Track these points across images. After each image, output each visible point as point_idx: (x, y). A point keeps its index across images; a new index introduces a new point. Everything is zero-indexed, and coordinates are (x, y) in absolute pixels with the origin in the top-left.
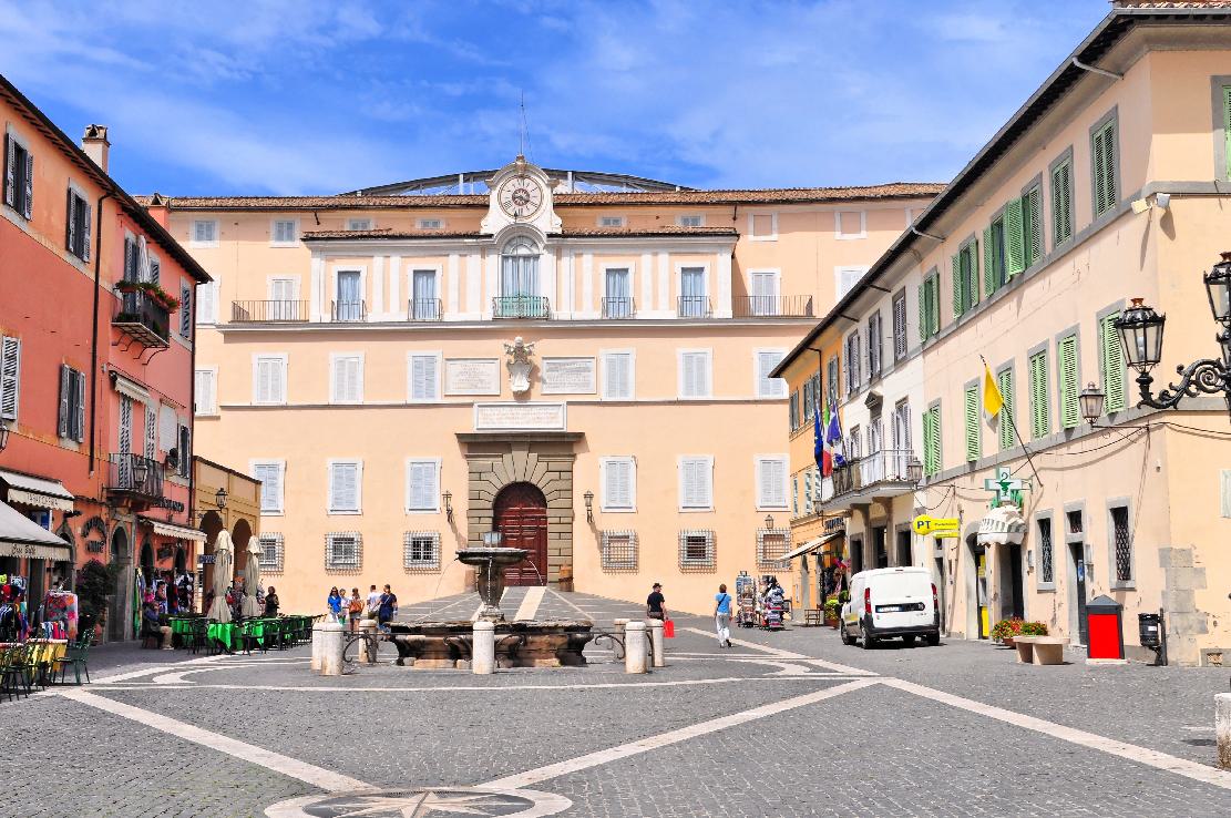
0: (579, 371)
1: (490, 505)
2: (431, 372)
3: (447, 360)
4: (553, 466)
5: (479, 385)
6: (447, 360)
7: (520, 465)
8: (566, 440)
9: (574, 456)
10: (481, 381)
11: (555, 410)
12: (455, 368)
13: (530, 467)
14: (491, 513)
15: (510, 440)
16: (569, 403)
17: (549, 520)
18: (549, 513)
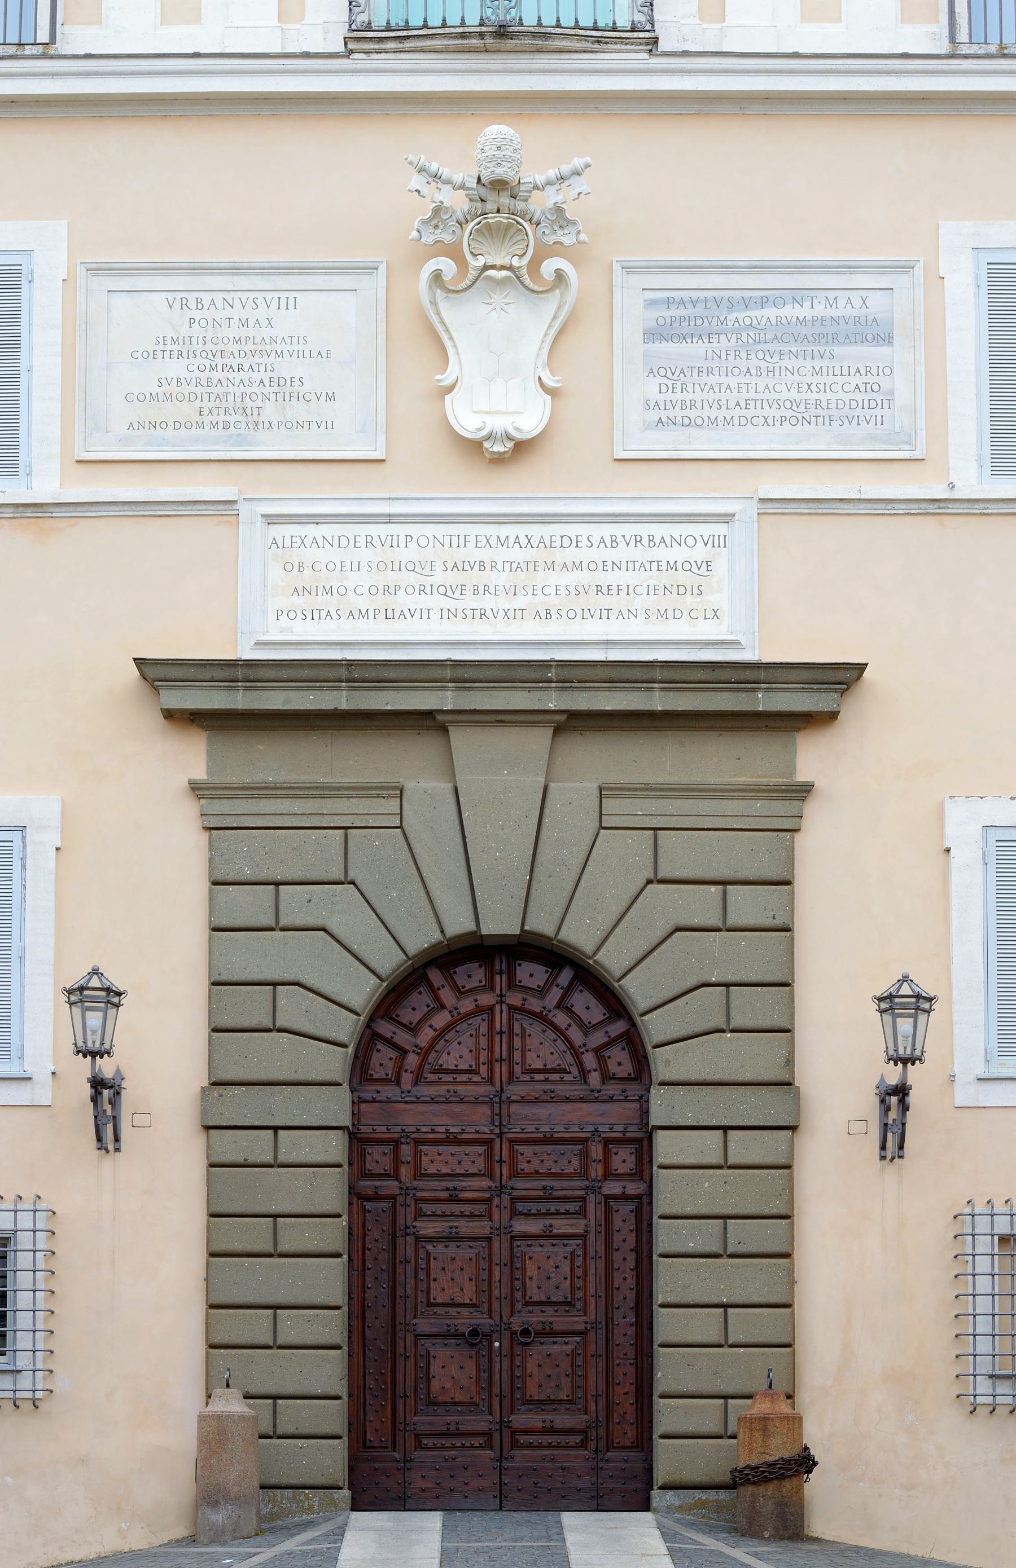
0: (826, 334)
1: (334, 1063)
3: (98, 270)
4: (681, 855)
5: (270, 411)
6: (98, 270)
7: (501, 853)
8: (763, 701)
9: (805, 791)
10: (285, 390)
11: (688, 546)
12: (141, 316)
13: (562, 852)
15: (446, 700)
16: (773, 507)
17: (667, 1147)
18: (661, 1106)
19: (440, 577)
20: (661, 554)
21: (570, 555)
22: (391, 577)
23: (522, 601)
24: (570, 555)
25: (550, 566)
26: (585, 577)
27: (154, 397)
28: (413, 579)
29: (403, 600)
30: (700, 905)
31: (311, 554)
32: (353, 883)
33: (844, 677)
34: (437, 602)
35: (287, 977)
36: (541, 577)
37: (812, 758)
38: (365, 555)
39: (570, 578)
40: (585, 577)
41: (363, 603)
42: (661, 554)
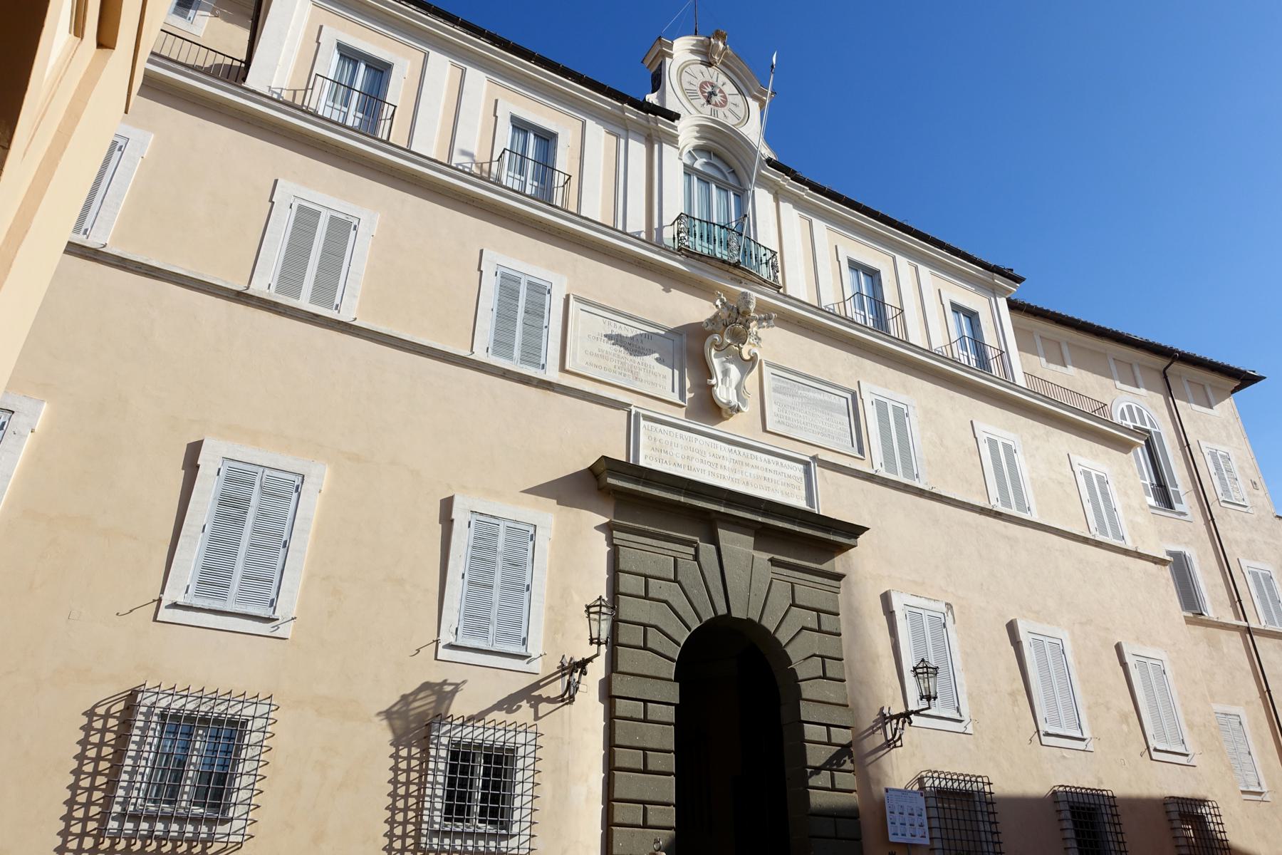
2: (536, 311)
5: (642, 374)
14: (672, 692)
19: (708, 458)
20: (784, 470)
21: (754, 462)
22: (690, 453)
23: (738, 476)
24: (754, 462)
25: (747, 465)
26: (760, 473)
27: (596, 355)
28: (698, 456)
29: (695, 464)
30: (810, 619)
31: (659, 436)
32: (679, 583)
33: (855, 531)
34: (707, 468)
35: (652, 622)
36: (745, 468)
37: (837, 564)
38: (680, 441)
39: (754, 471)
40: (760, 473)
41: (679, 461)
42: (784, 470)
